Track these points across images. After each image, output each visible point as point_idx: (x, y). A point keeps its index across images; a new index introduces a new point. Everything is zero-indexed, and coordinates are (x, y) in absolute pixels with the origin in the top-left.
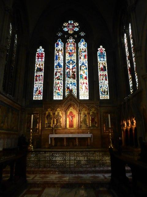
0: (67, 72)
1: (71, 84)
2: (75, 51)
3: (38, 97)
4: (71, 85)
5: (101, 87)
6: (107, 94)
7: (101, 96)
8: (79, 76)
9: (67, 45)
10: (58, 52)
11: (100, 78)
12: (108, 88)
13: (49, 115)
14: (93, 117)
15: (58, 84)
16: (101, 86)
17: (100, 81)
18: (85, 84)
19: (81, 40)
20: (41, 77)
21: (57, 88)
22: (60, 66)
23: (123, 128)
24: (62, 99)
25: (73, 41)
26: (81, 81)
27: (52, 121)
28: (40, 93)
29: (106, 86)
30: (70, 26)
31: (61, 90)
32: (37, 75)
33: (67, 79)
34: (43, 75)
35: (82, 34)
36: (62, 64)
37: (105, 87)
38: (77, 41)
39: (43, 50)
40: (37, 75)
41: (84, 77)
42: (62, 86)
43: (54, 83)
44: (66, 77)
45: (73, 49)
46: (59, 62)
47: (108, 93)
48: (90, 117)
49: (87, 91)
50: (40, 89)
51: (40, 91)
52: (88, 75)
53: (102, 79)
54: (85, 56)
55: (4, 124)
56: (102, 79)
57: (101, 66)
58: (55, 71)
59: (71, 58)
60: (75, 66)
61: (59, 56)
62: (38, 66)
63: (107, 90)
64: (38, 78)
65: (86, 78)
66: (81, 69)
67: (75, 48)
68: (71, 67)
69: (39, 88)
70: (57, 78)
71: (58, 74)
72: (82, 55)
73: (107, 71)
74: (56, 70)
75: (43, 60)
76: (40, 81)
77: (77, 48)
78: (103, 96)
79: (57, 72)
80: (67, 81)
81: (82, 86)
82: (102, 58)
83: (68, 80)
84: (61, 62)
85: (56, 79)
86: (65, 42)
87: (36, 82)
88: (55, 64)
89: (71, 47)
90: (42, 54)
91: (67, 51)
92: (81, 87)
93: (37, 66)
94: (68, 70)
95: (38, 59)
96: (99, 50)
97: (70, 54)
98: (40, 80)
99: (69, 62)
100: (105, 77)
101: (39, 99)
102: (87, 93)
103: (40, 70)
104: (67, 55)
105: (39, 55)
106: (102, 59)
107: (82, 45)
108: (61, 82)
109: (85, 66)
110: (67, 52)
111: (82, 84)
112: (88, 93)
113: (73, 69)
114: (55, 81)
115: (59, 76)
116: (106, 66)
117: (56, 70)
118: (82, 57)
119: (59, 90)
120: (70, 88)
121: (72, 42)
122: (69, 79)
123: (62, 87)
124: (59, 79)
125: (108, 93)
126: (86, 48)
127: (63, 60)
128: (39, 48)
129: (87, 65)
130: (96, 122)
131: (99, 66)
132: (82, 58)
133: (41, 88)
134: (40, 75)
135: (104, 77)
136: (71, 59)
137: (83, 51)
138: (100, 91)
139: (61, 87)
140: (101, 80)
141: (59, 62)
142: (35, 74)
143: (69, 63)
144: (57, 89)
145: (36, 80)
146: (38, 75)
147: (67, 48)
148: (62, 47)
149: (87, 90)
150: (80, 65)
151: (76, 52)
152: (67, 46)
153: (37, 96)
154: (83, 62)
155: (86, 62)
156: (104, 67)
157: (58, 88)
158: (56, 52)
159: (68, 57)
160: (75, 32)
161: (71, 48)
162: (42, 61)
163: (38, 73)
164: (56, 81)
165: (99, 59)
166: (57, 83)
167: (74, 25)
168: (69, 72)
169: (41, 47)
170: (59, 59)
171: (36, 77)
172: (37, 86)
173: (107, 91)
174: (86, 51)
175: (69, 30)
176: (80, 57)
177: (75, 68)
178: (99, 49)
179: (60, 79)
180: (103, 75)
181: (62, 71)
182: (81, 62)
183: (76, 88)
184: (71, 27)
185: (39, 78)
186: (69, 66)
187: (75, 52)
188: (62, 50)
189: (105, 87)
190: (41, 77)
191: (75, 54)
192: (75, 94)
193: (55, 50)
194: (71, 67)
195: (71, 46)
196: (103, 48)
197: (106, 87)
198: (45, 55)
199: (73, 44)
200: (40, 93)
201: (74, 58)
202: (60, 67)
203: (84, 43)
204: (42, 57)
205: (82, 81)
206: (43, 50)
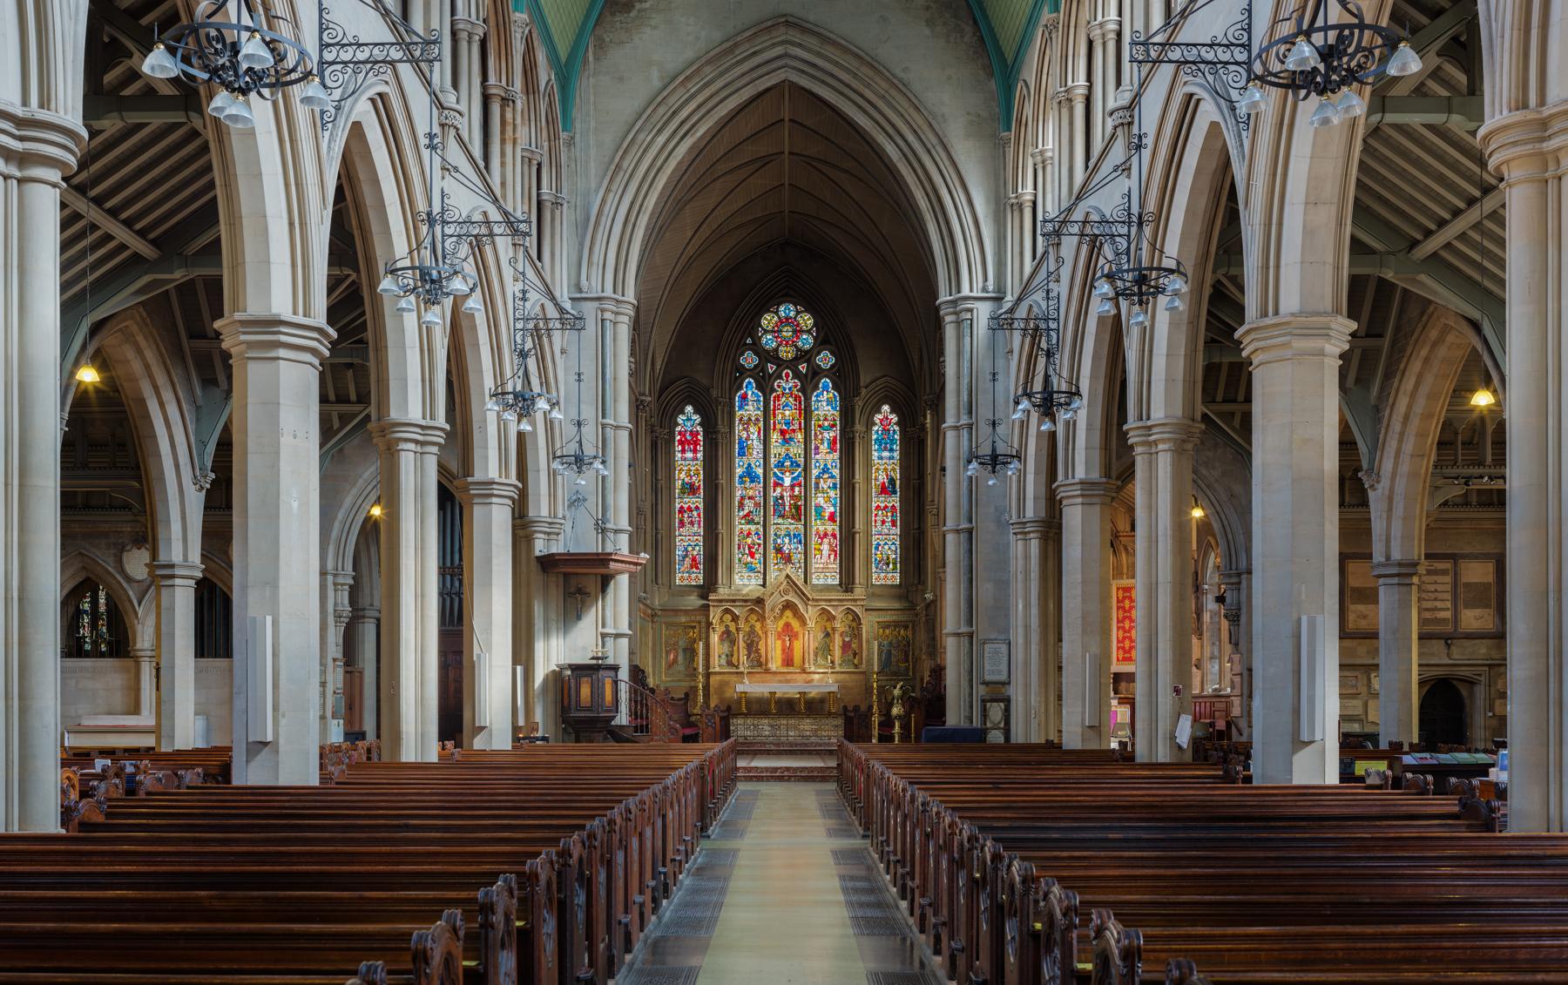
0: (777, 499)
22: (753, 478)
26: (818, 526)
33: (773, 520)
35: (825, 359)
36: (760, 471)
38: (809, 383)
51: (694, 559)
53: (883, 522)
56: (883, 522)
57: (882, 478)
58: (738, 493)
62: (683, 476)
65: (832, 518)
66: (817, 487)
68: (787, 482)
71: (749, 505)
75: (700, 455)
77: (807, 413)
79: (742, 498)
88: (739, 471)
89: (787, 413)
93: (681, 477)
94: (779, 490)
95: (683, 451)
99: (780, 465)
104: (775, 436)
106: (886, 454)
109: (833, 477)
112: (836, 566)
113: (792, 487)
129: (836, 472)
132: (824, 448)
150: (815, 472)
156: (892, 481)
158: (738, 428)
159: (777, 448)
164: (740, 526)
168: (782, 497)
169: (689, 409)
174: (833, 426)
176: (817, 448)
178: (879, 416)
191: (800, 436)
194: (787, 482)
201: (796, 450)
204: (696, 443)
205: (821, 529)
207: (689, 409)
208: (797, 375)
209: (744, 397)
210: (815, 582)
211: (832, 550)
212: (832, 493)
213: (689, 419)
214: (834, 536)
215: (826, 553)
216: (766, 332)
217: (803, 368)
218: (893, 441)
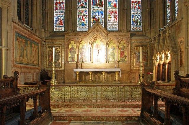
1: (98, 13)
3: (59, 28)
4: (97, 14)
5: (133, 17)
6: (140, 25)
7: (132, 27)
8: (108, 3)
13: (73, 48)
14: (122, 51)
15: (82, 12)
16: (133, 16)
17: (132, 9)
18: (114, 13)
20: (62, 4)
23: (155, 63)
26: (109, 9)
27: (76, 55)
29: (139, 15)
32: (57, 2)
33: (92, 6)
37: (138, 17)
40: (57, 2)
41: (113, 4)
43: (78, 11)
44: (92, 4)
47: (141, 23)
48: (119, 51)
50: (61, 19)
52: (117, 2)
53: (135, 7)
55: (23, 58)
56: (135, 7)
63: (139, 20)
64: (58, 5)
65: (115, 6)
69: (59, 17)
70: (81, 5)
76: (61, 9)
81: (111, 15)
83: (94, 8)
85: (80, 7)
87: (56, 10)
92: (109, 16)
98: (60, 8)
100: (139, 5)
101: (61, 31)
102: (116, 24)
111: (111, 12)
112: (117, 24)
115: (83, 4)
119: (83, 19)
120: (97, 17)
122: (95, 7)
123: (86, 16)
124: (83, 7)
125: (141, 23)
130: (125, 56)
133: (62, 17)
134: (61, 2)
135: (136, 5)
138: (131, 21)
139: (85, 16)
140: (133, 8)
142: (55, 1)
144: (82, 18)
145: (57, 9)
146: (59, 2)
149: (116, 20)
157: (83, 17)
164: (80, 9)
166: (81, 11)
171: (56, 4)
172: (58, 16)
179: (84, 7)
183: (103, 17)
189: (138, 17)
200: (61, 23)
205: (111, 10)
214: (116, 12)
215: (113, 19)
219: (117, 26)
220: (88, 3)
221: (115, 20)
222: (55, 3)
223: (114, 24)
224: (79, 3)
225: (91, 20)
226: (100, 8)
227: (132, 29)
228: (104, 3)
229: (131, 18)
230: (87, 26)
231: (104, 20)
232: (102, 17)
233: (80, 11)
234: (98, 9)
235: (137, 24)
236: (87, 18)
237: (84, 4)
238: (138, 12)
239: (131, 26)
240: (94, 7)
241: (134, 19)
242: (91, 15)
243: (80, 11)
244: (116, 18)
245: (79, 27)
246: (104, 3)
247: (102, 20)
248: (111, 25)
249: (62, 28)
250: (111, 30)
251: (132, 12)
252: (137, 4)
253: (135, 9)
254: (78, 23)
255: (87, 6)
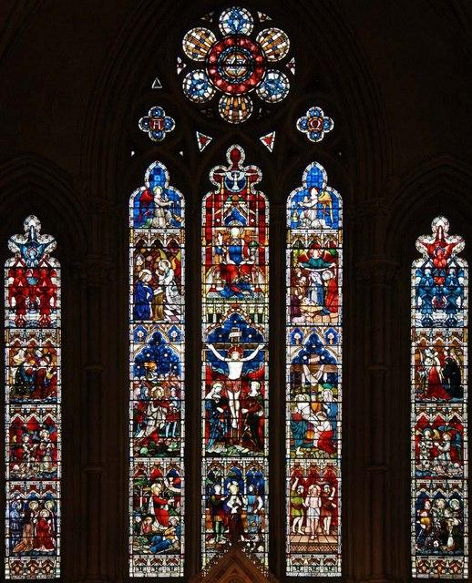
2: (262, 254)
4: (234, 489)
5: (420, 506)
7: (415, 561)
9: (209, 211)
10: (147, 265)
11: (421, 442)
12: (466, 511)
15: (154, 479)
16: (423, 498)
19: (305, 177)
20: (45, 434)
21: (146, 506)
24: (179, 572)
25: (253, 179)
26: (297, 459)
28: (43, 537)
29: (455, 496)
30: (232, 60)
31: (173, 520)
32: (18, 422)
33: (208, 447)
34: (57, 419)
35: (315, 124)
37: (447, 506)
38: (280, 178)
39: (49, 249)
40: (18, 422)
42: (181, 491)
45: (248, 245)
46: (157, 337)
49: (333, 527)
51: (42, 526)
53: (434, 453)
54: (327, 293)
56: (434, 453)
58: (135, 394)
59: (237, 307)
60: (258, 359)
61: (157, 292)
62: (19, 358)
63: (456, 522)
64: (27, 439)
67: (262, 233)
68: (235, 370)
69: (34, 506)
71: (156, 419)
72: (307, 286)
73: (466, 396)
74: (138, 391)
75: (55, 317)
76: (41, 461)
77: (278, 231)
78: (432, 560)
79: (144, 403)
80: (210, 460)
81: (304, 496)
82: (439, 306)
83: (214, 455)
84: (174, 334)
85: (144, 450)
86: (192, 181)
88: (136, 349)
89: (235, 231)
90: (43, 274)
91: (209, 252)
92: (296, 501)
95: (20, 309)
96: (423, 250)
97: (229, 280)
99: (220, 337)
100: (452, 441)
101: (41, 576)
103: (34, 385)
104: (209, 279)
105: (27, 284)
107: (312, 214)
108: (173, 465)
109: (328, 361)
110: (208, 266)
114: (137, 460)
115: (159, 431)
116: (466, 363)
117: (138, 391)
118: (306, 301)
119: (160, 516)
120: (230, 504)
121: (241, 184)
123: (177, 496)
124: (160, 450)
126: (334, 232)
127: (182, 318)
128: (21, 232)
129: (336, 352)
131: (420, 366)
132: (310, 304)
133: (50, 505)
135: (441, 440)
136: (235, 316)
137: (316, 254)
138: (413, 528)
140: (424, 456)
141: (157, 337)
143: (225, 338)
147: (209, 234)
148: (176, 224)
149: (334, 520)
150: (292, 352)
151: (267, 261)
152: (209, 219)
153: (28, 559)
154: (314, 337)
155: (331, 336)
156: (452, 369)
157: (157, 505)
160: (268, 116)
161: (235, 232)
162: (49, 326)
163: (29, 407)
164: (140, 461)
165: (418, 316)
167: (260, 50)
169: (33, 222)
170: (161, 315)
173: (459, 528)
174: (334, 258)
175: (218, 95)
176: (296, 303)
177: (261, 379)
178: (423, 244)
180: (438, 423)
181: (178, 392)
182: (297, 336)
184: (235, 65)
185: (32, 442)
186: (225, 365)
187: (262, 264)
188: (174, 246)
190: (45, 434)
191: (262, 280)
192: (261, 543)
193: (132, 250)
194: (235, 370)
195: (234, 217)
196: (451, 233)
197: (455, 505)
198: (63, 279)
199: (252, 207)
200: (43, 537)
201: (255, 307)
202: (162, 370)
203: (326, 197)
206: (48, 241)
207: (33, 222)
208: (256, 155)
209: (147, 202)
210: (291, 572)
211: (326, 508)
212: (327, 395)
213: (32, 244)
214: (331, 480)
216: (192, 66)
217: (268, 141)
218: (454, 291)
219: (335, 553)
220: (183, 428)
221: (327, 522)
222: (7, 427)
223: (319, 544)
224: (135, 430)
225: (203, 522)
226: (246, 455)
227: (414, 570)
228: (266, 430)
229: (413, 510)
230: (179, 552)
231: (267, 522)
232: (257, 503)
233: (141, 472)
234: (236, 464)
235: (445, 543)
236: (181, 508)
237: (163, 431)
238: (447, 478)
239: (413, 551)
240: (218, 451)
241: (425, 514)
242: (203, 492)
243: (141, 472)
244: (333, 511)
245: (137, 557)
246: (266, 430)
247: (259, 519)
248: (303, 549)
249: (48, 562)
250: (305, 572)
251: (417, 478)
252: (446, 437)
253: (436, 462)
254: (131, 538)
255: (179, 443)
